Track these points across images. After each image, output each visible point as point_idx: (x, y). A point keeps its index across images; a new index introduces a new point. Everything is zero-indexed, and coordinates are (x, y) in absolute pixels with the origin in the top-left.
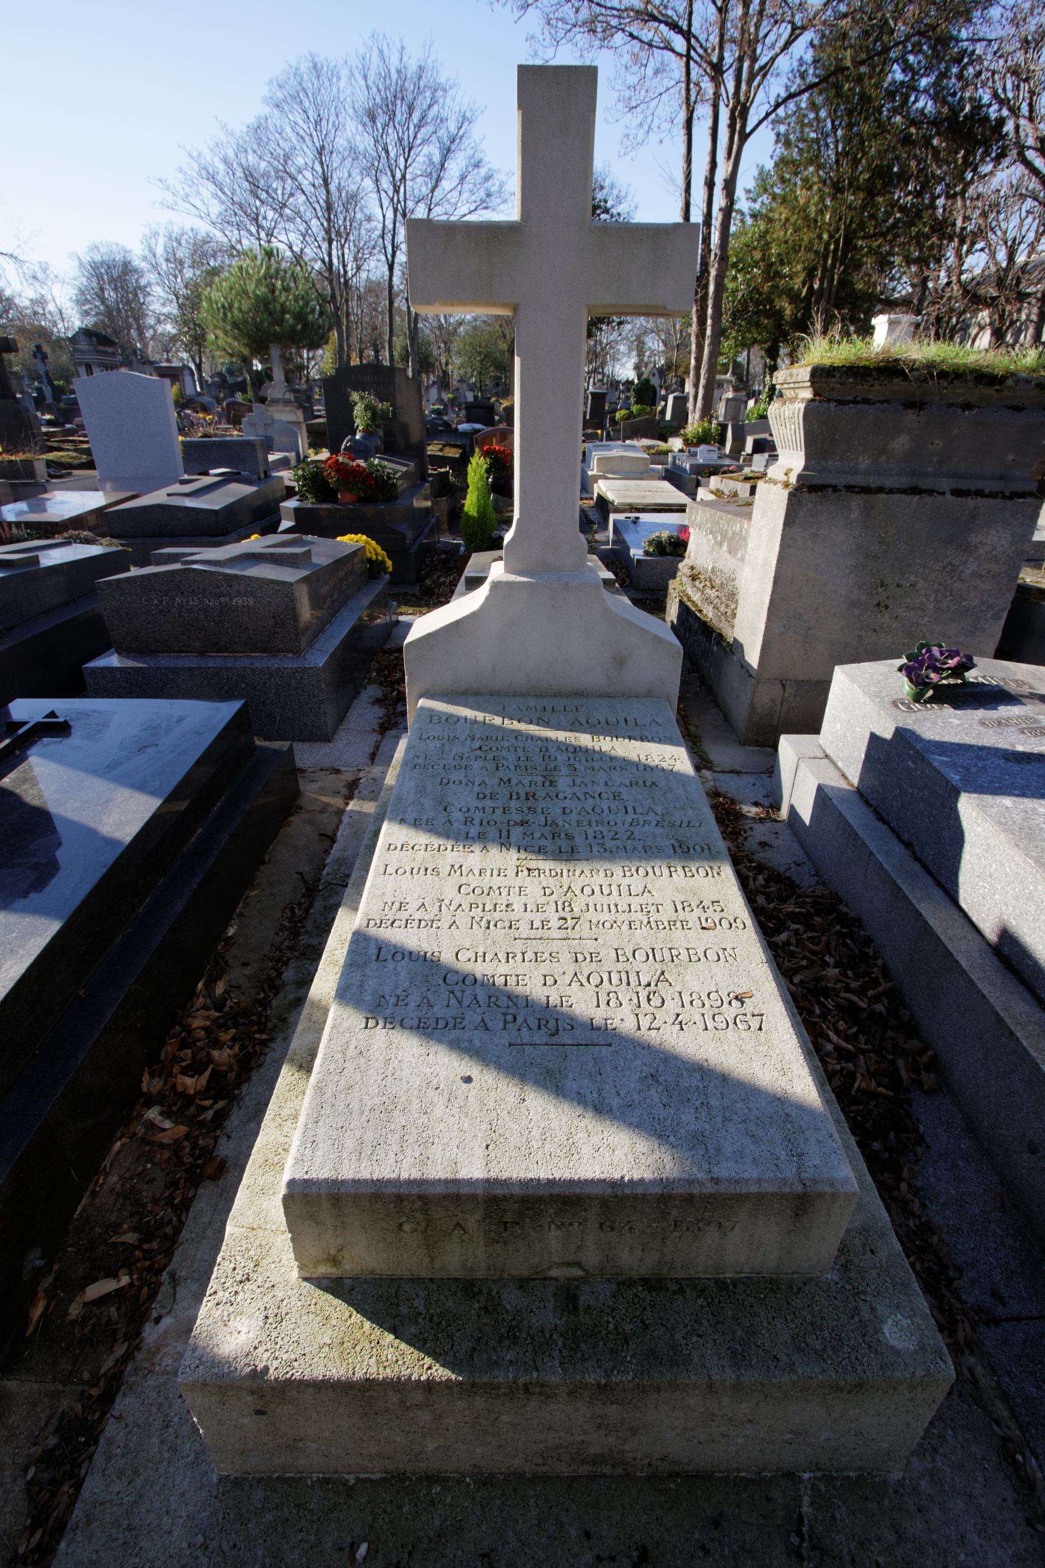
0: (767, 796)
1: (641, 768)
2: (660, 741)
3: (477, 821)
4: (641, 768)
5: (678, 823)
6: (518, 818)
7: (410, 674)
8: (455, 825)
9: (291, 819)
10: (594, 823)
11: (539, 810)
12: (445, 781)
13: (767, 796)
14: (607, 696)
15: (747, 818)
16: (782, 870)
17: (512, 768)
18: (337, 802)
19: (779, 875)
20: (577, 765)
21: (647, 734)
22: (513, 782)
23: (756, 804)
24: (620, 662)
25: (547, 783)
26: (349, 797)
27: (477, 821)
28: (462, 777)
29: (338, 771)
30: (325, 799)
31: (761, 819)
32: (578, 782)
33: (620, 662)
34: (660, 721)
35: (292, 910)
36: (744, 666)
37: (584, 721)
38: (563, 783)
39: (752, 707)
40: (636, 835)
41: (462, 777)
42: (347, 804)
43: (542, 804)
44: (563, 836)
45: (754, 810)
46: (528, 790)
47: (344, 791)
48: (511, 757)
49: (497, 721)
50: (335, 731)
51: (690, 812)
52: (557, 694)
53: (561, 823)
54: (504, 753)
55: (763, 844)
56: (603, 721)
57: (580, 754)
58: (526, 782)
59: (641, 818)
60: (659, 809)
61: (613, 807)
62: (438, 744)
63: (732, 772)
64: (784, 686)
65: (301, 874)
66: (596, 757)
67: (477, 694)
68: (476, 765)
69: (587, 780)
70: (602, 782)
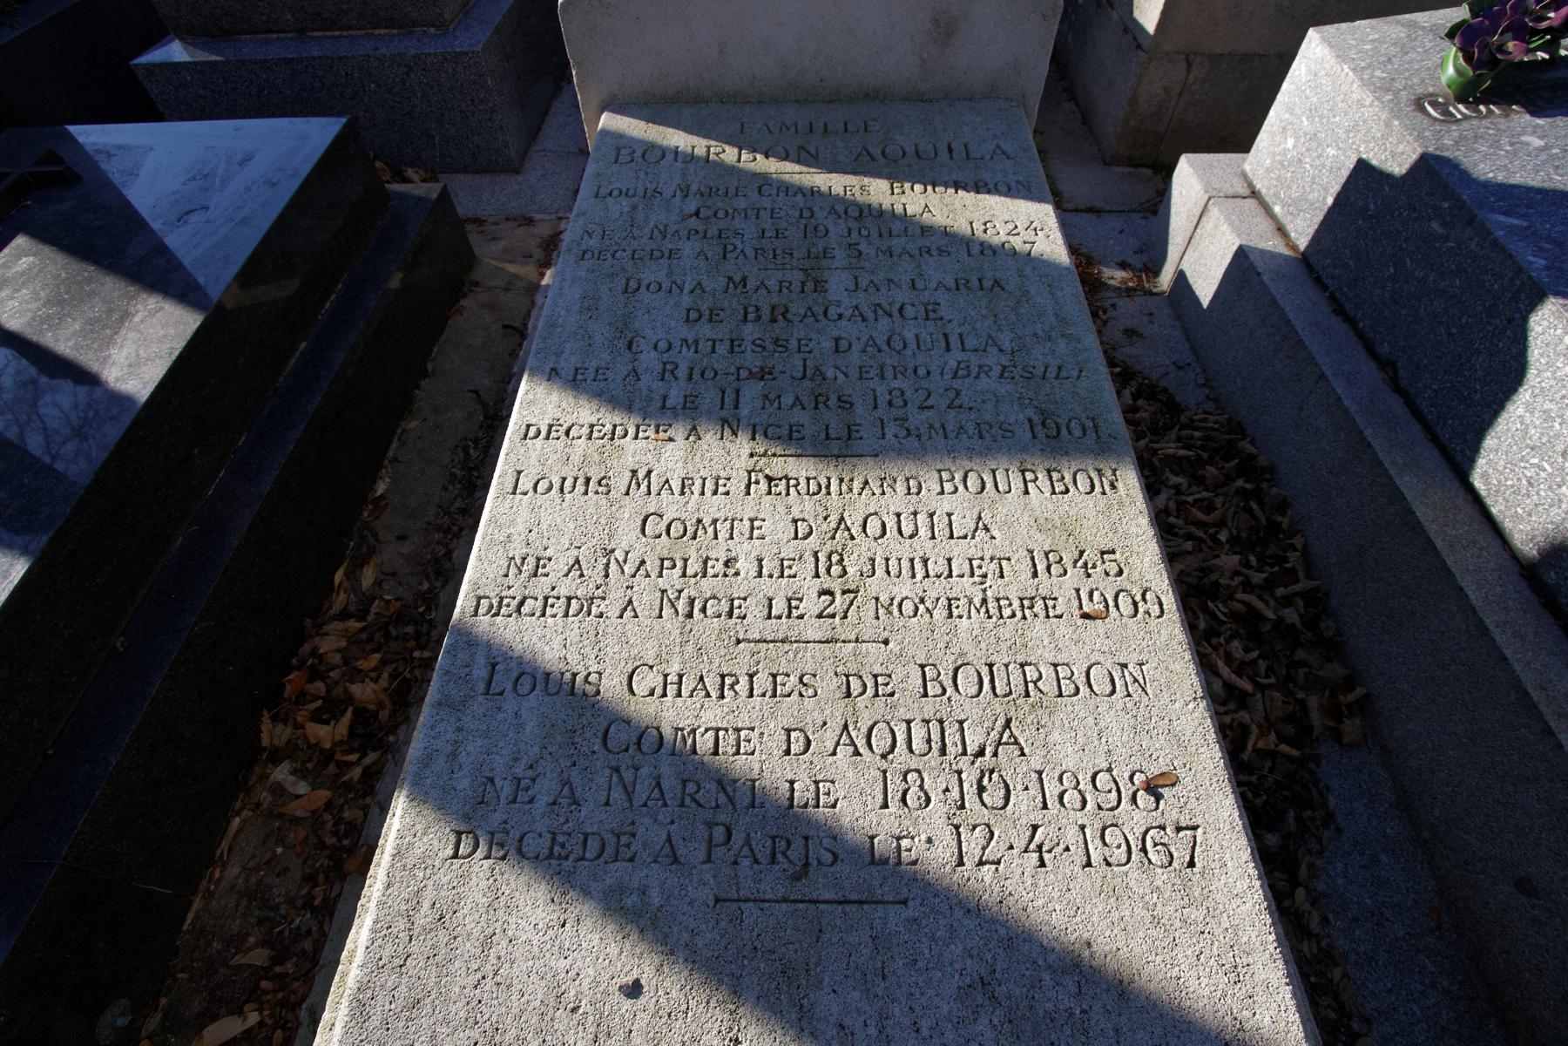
0: (1139, 252)
1: (976, 250)
2: (1009, 192)
3: (682, 372)
4: (976, 250)
5: (1039, 371)
6: (753, 361)
7: (579, 65)
8: (645, 379)
9: (463, 302)
10: (889, 373)
11: (794, 343)
12: (633, 284)
13: (1139, 252)
14: (917, 98)
15: (1109, 287)
16: (1155, 376)
17: (750, 253)
18: (527, 271)
19: (1153, 386)
20: (863, 247)
21: (987, 176)
22: (751, 284)
23: (1123, 265)
24: (945, 29)
25: (810, 285)
26: (546, 264)
27: (682, 372)
28: (661, 276)
29: (530, 222)
30: (511, 268)
31: (1129, 290)
32: (863, 283)
33: (945, 29)
34: (1009, 150)
35: (466, 450)
36: (1132, 28)
37: (877, 152)
38: (838, 283)
39: (1133, 102)
40: (965, 399)
41: (661, 276)
42: (543, 275)
43: (799, 332)
44: (833, 401)
45: (1120, 275)
46: (775, 300)
47: (538, 254)
48: (750, 230)
49: (730, 154)
50: (524, 153)
51: (1062, 347)
52: (836, 98)
53: (830, 374)
54: (738, 223)
55: (1131, 333)
56: (910, 150)
57: (869, 222)
58: (772, 283)
59: (974, 360)
60: (1005, 340)
61: (924, 335)
62: (625, 204)
63: (1090, 210)
64: (1189, 65)
65: (476, 392)
66: (897, 227)
67: (697, 100)
68: (688, 248)
69: (879, 278)
70: (906, 279)
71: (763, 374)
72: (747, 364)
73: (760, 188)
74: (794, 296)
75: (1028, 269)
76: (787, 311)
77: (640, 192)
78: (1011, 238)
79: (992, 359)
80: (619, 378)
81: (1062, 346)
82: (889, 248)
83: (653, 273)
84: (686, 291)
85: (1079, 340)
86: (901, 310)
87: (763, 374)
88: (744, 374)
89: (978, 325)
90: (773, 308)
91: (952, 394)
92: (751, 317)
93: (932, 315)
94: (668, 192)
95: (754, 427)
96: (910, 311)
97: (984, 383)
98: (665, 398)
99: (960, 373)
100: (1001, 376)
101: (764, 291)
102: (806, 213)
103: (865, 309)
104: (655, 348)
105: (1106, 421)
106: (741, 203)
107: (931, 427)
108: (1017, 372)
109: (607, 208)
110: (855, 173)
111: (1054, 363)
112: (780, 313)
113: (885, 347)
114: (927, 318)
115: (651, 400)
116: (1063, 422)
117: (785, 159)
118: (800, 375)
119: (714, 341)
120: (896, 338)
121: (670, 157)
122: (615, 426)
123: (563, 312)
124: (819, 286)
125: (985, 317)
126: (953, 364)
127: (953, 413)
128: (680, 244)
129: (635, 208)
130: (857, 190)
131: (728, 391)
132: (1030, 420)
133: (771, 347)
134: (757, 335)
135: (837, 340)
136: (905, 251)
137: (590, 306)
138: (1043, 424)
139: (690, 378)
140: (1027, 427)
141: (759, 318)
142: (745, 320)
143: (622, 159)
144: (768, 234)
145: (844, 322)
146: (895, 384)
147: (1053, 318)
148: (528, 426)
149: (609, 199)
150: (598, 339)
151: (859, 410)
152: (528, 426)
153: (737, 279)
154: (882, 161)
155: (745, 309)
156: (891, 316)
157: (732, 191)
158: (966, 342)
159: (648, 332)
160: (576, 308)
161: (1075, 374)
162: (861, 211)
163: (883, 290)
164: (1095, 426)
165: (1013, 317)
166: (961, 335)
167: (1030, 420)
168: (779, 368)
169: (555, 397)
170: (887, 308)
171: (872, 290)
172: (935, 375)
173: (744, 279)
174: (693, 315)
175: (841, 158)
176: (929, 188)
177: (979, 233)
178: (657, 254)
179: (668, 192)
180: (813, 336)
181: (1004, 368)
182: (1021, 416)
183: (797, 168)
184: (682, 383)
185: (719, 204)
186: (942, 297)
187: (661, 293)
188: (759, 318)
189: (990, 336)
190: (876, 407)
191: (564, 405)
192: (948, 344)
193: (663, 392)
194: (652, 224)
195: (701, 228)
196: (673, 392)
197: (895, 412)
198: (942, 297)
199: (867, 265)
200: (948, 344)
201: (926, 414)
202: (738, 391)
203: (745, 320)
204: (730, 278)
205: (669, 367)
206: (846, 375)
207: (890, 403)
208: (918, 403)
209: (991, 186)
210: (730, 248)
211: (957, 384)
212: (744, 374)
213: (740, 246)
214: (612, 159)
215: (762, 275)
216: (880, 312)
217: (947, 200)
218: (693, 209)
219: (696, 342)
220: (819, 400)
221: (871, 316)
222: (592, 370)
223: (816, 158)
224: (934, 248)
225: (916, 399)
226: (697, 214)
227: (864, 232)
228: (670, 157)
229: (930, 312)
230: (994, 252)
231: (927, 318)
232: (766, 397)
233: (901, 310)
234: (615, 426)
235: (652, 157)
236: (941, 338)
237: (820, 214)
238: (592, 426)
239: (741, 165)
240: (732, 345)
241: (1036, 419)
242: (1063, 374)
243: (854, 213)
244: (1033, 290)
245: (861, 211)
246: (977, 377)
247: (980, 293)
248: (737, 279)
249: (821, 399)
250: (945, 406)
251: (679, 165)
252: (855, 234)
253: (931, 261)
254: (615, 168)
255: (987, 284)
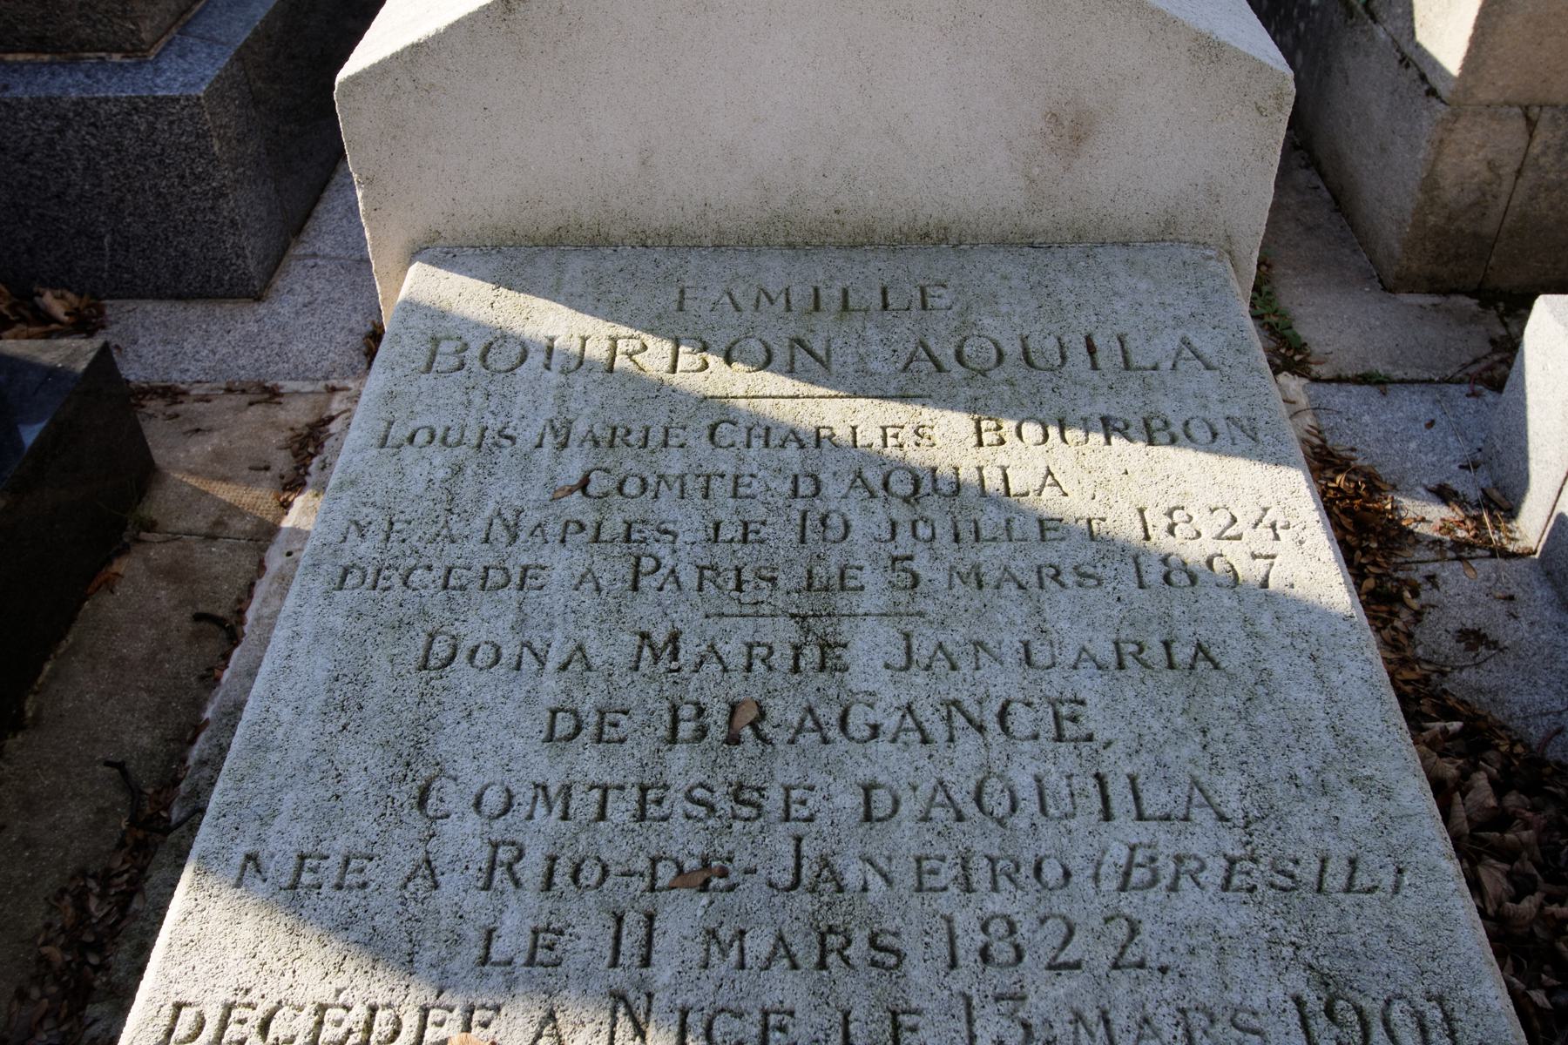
0: (1471, 466)
1: (1154, 575)
2: (1213, 441)
3: (531, 869)
4: (1154, 575)
5: (1307, 873)
6: (685, 840)
7: (369, 182)
8: (451, 883)
9: (120, 566)
10: (981, 877)
11: (775, 796)
12: (441, 649)
13: (1471, 466)
14: (1023, 242)
15: (1417, 540)
16: (1535, 734)
17: (689, 577)
18: (256, 498)
19: (1536, 761)
20: (920, 565)
21: (1167, 407)
22: (689, 650)
23: (1443, 494)
24: (1072, 130)
25: (811, 654)
26: (295, 484)
27: (531, 869)
28: (502, 631)
29: (272, 395)
30: (225, 493)
31: (1459, 545)
32: (923, 651)
33: (1072, 130)
35: (81, 898)
36: (1413, 63)
37: (946, 354)
38: (869, 647)
39: (1430, 185)
40: (1149, 945)
41: (502, 631)
42: (286, 506)
43: (786, 768)
44: (858, 950)
45: (1437, 513)
46: (738, 688)
47: (283, 462)
48: (688, 521)
49: (655, 356)
50: (275, 263)
51: (1353, 809)
52: (861, 241)
53: (852, 878)
54: (667, 508)
55: (1473, 638)
56: (1012, 349)
57: (932, 507)
58: (733, 650)
59: (1166, 841)
60: (1229, 791)
61: (1053, 779)
62: (440, 458)
63: (1364, 379)
64: (1531, 124)
65: (120, 766)
66: (990, 520)
67: (596, 242)
68: (562, 564)
69: (955, 638)
70: (1010, 643)
71: (706, 876)
72: (674, 850)
73: (713, 429)
74: (777, 679)
75: (1265, 620)
76: (762, 715)
77: (472, 436)
78: (1224, 546)
79: (1206, 841)
80: (395, 881)
81: (1353, 807)
82: (976, 567)
83: (486, 621)
84: (551, 666)
85: (1387, 793)
86: (1003, 715)
87: (706, 876)
88: (666, 873)
89: (1169, 755)
90: (734, 708)
91: (1120, 931)
92: (686, 729)
93: (1069, 729)
94: (528, 436)
95: (684, 1013)
96: (1021, 720)
97: (1193, 903)
98: (490, 935)
99: (1138, 875)
100: (1226, 886)
101: (713, 667)
102: (805, 487)
103: (925, 712)
104: (478, 804)
105: (1470, 1004)
106: (674, 463)
107: (1078, 1017)
108: (1261, 872)
109: (402, 472)
110: (904, 397)
111: (1340, 852)
112: (746, 723)
113: (970, 809)
114: (1060, 738)
115: (458, 940)
116: (1373, 1007)
117: (766, 364)
118: (787, 878)
119: (605, 790)
120: (993, 785)
121: (535, 359)
122: (373, 1010)
123: (287, 715)
124: (830, 655)
125: (1180, 734)
126: (1119, 853)
127: (1122, 983)
128: (546, 555)
129: (458, 470)
130: (907, 435)
131: (631, 918)
132: (1299, 1001)
133: (724, 805)
134: (697, 776)
135: (868, 789)
136: (1008, 575)
137: (345, 703)
138: (1329, 1012)
139: (549, 884)
140: (1293, 1018)
141: (702, 732)
142: (673, 739)
143: (442, 363)
144: (726, 534)
145: (883, 746)
146: (995, 904)
147: (1327, 739)
148: (178, 1007)
149: (409, 453)
150: (357, 782)
151: (918, 972)
152: (178, 1007)
153: (660, 637)
154: (957, 372)
155: (674, 710)
156: (981, 729)
157: (657, 436)
158: (1145, 797)
159: (465, 767)
160: (315, 704)
161: (1388, 879)
162: (917, 482)
163: (965, 666)
164: (1448, 1018)
165: (1242, 736)
166: (1133, 779)
167: (1299, 1001)
168: (743, 859)
169: (247, 929)
170: (974, 710)
171: (941, 666)
172: (1082, 879)
173: (674, 638)
174: (564, 725)
175: (874, 366)
176: (1053, 431)
177: (1161, 541)
178: (496, 577)
179: (528, 436)
180: (817, 778)
181: (1232, 862)
182: (1277, 992)
183: (787, 385)
184: (531, 895)
185: (630, 464)
186: (1087, 684)
187: (499, 670)
188: (702, 732)
189: (1195, 782)
190: (953, 965)
191: (265, 952)
192: (1105, 799)
193: (484, 920)
194: (490, 508)
195: (589, 519)
196: (509, 922)
197: (1004, 980)
198: (1087, 684)
199: (929, 606)
200: (1105, 799)
201: (1069, 983)
202: (651, 918)
203: (673, 739)
204: (645, 636)
205: (504, 854)
206: (889, 881)
207: (985, 955)
208: (1046, 955)
209: (1177, 429)
210: (648, 564)
211: (1130, 904)
212: (666, 873)
213: (668, 561)
214: (422, 364)
215: (713, 628)
216: (960, 721)
217: (1090, 460)
218: (575, 476)
219: (567, 790)
220: (829, 943)
221: (938, 730)
222: (335, 861)
223: (824, 363)
224: (1067, 568)
225: (1042, 942)
226: (584, 485)
227: (924, 531)
228: (535, 359)
229: (1064, 721)
230: (1193, 579)
231: (1060, 738)
232: (712, 933)
233: (1003, 715)
234: (373, 1010)
235: (499, 360)
236: (1091, 787)
237: (832, 489)
238: (322, 1008)
239: (677, 379)
240: (643, 802)
241: (1314, 1004)
242: (1362, 880)
243: (902, 487)
244: (1279, 670)
245: (917, 482)
246: (1173, 888)
247: (1169, 677)
248: (660, 637)
249: (834, 941)
250: (1106, 964)
251: (554, 377)
252: (904, 533)
253: (1062, 598)
254: (426, 381)
255: (1183, 654)
